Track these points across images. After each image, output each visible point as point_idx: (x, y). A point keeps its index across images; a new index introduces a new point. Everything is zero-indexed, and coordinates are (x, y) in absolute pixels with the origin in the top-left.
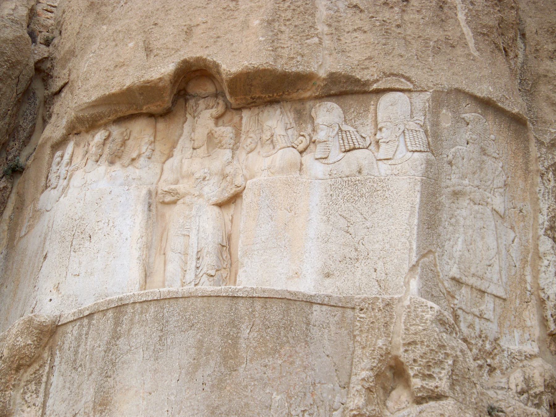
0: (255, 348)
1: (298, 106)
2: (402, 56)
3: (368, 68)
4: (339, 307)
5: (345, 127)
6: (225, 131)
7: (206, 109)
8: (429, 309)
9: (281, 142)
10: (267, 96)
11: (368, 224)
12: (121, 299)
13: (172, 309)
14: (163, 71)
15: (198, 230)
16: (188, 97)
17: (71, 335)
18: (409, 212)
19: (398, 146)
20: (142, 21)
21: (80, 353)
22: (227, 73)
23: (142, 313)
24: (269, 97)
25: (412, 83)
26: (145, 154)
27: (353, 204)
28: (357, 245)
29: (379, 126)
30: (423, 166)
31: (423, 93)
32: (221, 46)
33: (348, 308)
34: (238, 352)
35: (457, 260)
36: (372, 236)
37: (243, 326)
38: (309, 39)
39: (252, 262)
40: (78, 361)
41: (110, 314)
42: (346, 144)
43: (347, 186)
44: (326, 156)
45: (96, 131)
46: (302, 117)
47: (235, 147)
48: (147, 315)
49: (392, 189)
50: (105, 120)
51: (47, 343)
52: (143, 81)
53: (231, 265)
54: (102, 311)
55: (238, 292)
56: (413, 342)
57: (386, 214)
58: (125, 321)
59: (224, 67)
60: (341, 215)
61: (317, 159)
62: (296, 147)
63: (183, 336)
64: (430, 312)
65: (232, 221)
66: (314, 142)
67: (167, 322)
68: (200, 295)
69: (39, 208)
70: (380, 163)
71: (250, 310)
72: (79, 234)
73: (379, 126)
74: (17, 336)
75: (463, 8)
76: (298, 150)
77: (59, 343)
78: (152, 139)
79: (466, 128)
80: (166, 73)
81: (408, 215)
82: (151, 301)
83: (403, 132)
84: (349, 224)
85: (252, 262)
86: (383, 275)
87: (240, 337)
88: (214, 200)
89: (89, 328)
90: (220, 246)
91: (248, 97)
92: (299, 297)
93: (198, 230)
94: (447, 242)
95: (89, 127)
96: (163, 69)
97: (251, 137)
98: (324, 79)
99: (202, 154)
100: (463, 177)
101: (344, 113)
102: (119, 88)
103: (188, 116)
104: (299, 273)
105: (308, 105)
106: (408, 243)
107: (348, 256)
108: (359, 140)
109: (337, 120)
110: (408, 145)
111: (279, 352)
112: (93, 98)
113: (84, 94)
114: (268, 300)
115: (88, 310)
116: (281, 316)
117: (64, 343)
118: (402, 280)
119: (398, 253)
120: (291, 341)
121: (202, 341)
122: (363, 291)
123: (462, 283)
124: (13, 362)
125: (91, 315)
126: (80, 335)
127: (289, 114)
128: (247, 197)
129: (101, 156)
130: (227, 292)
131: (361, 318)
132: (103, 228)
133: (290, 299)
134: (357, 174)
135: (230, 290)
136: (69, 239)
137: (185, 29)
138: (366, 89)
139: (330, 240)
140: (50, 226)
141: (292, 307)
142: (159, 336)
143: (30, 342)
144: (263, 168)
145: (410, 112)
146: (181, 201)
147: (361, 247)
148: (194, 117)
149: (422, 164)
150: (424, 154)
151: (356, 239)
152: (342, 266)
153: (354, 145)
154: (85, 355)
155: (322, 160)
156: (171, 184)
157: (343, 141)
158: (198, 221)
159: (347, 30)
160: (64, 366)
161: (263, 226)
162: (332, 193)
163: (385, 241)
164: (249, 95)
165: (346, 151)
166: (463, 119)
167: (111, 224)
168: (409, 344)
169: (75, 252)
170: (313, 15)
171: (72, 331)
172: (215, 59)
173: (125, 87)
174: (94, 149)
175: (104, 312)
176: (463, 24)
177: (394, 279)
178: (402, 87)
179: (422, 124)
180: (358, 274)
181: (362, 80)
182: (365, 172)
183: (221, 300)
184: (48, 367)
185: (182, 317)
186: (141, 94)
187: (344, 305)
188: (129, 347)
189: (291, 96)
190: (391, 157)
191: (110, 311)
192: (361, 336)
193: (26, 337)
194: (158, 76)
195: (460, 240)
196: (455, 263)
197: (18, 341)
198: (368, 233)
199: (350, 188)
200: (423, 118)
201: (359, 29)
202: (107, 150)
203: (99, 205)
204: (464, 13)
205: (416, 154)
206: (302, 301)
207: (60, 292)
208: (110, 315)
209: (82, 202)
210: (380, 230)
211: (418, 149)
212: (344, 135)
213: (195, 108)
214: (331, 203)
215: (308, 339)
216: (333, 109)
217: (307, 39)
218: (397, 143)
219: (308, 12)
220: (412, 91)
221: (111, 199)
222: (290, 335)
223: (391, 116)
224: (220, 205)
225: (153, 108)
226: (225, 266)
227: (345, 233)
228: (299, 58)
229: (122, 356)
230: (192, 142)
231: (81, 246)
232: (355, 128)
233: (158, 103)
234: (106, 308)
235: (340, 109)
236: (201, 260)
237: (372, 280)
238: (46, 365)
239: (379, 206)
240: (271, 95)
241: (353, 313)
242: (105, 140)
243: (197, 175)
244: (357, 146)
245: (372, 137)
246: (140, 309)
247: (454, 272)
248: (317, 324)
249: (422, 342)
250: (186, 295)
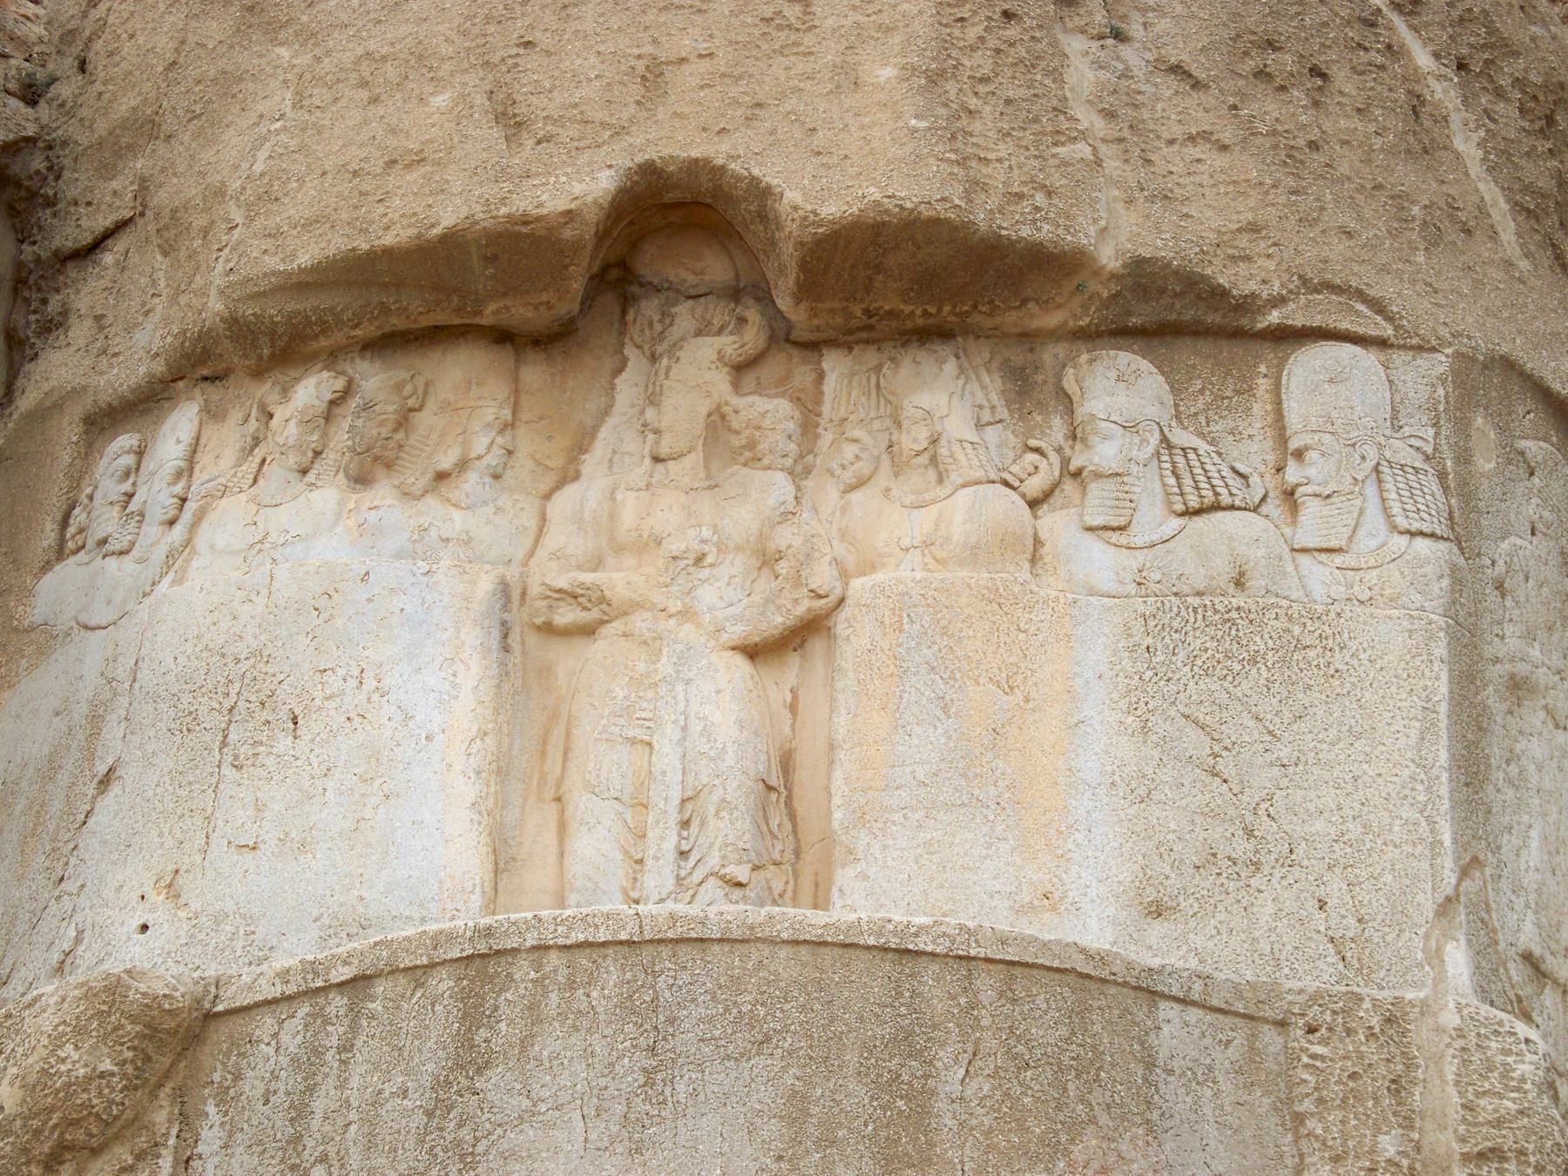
0: (988, 1133)
1: (1016, 355)
2: (1349, 235)
3: (1248, 258)
4: (1237, 1014)
5: (1180, 437)
6: (770, 412)
7: (699, 333)
8: (1523, 1046)
9: (967, 464)
10: (918, 312)
11: (1285, 753)
12: (488, 932)
13: (685, 977)
14: (578, 189)
15: (684, 729)
16: (635, 289)
17: (271, 1050)
18: (1417, 725)
19: (1362, 511)
20: (475, 30)
21: (319, 1115)
22: (805, 218)
23: (572, 985)
24: (926, 314)
25: (1390, 319)
26: (484, 462)
27: (1226, 684)
28: (1250, 818)
29: (1294, 444)
30: (1445, 582)
31: (1425, 355)
32: (773, 132)
33: (1265, 1020)
34: (931, 1144)
35: (1532, 897)
36: (1300, 793)
37: (941, 1054)
38: (1063, 144)
39: (885, 847)
40: (310, 1143)
41: (442, 983)
42: (1187, 489)
43: (1200, 623)
44: (1122, 521)
45: (293, 373)
46: (1030, 391)
47: (799, 468)
48: (594, 994)
49: (1353, 645)
50: (338, 337)
51: (167, 1075)
52: (509, 216)
53: (797, 853)
54: (406, 969)
55: (916, 935)
56: (1492, 1150)
57: (1342, 724)
58: (504, 1009)
59: (792, 196)
60: (1187, 717)
61: (1090, 529)
62: (1017, 484)
63: (733, 1074)
64: (1529, 1057)
65: (793, 708)
66: (1077, 474)
67: (671, 1021)
68: (785, 936)
69: (38, 619)
70: (1304, 560)
71: (963, 1001)
72: (244, 710)
73: (1294, 444)
74: (57, 1042)
75: (1472, 126)
76: (1023, 496)
77: (216, 1077)
78: (507, 413)
79: (1529, 485)
80: (589, 199)
81: (1414, 734)
82: (604, 944)
83: (1376, 469)
84: (1217, 749)
85: (885, 847)
86: (1352, 921)
87: (933, 1093)
88: (737, 632)
89: (354, 1028)
90: (761, 785)
91: (857, 310)
92: (1115, 970)
93: (684, 729)
94: (1506, 836)
95: (272, 356)
96: (576, 184)
97: (855, 441)
98: (1113, 276)
99: (687, 480)
100: (1529, 637)
101: (1175, 390)
102: (412, 232)
103: (630, 351)
104: (1057, 895)
105: (1050, 354)
106: (1424, 824)
107: (1223, 850)
108: (1230, 482)
109: (1153, 411)
110: (1394, 511)
111: (1067, 1153)
112: (304, 260)
113: (267, 244)
114: (1017, 971)
115: (345, 963)
116: (1064, 1031)
117: (238, 1077)
118: (1418, 942)
119: (1391, 852)
120: (1103, 1119)
121: (804, 1097)
122: (1287, 971)
123: (1545, 975)
124: (37, 1132)
125: (359, 984)
126: (317, 1052)
127: (986, 378)
128: (856, 634)
129: (317, 454)
130: (880, 934)
131: (1314, 1057)
132: (343, 693)
133: (1088, 976)
134: (1231, 589)
135: (891, 927)
136: (219, 720)
137: (640, 66)
138: (1245, 322)
139: (1155, 796)
140: (122, 672)
141: (1095, 1004)
142: (645, 1070)
143: (107, 1065)
144: (906, 542)
145: (1389, 408)
146: (617, 626)
147: (1264, 826)
148: (654, 358)
149: (1442, 576)
150: (1442, 545)
151: (1245, 798)
152: (1205, 881)
153: (1217, 494)
154: (340, 1122)
155: (1110, 533)
156: (579, 568)
157: (1178, 477)
158: (681, 696)
159: (1166, 135)
161: (918, 730)
162: (1149, 641)
163: (1346, 812)
164: (862, 301)
165: (1190, 513)
166: (1522, 453)
167: (370, 683)
168: (1481, 1155)
169: (238, 768)
170: (1056, 75)
171: (275, 1035)
172: (756, 172)
173: (436, 231)
174: (293, 429)
175: (418, 974)
176: (1475, 170)
177: (1389, 938)
178: (1361, 330)
179: (1429, 449)
180: (1265, 912)
181: (1235, 292)
182: (1256, 583)
183: (860, 962)
184: (170, 1159)
185: (726, 1009)
186: (491, 260)
187: (1252, 1010)
188: (526, 1103)
189: (998, 320)
190: (1343, 543)
191: (444, 972)
192: (1322, 1119)
193: (95, 1047)
194: (562, 204)
195: (1533, 833)
196: (1527, 906)
197: (63, 1060)
198: (1284, 783)
199: (1211, 631)
200: (1431, 432)
201: (1205, 136)
202: (341, 437)
203: (324, 616)
204: (1475, 137)
205: (1420, 543)
206: (1125, 984)
207: (182, 901)
208: (443, 986)
209: (260, 600)
210: (1326, 775)
211: (1425, 527)
212: (1180, 460)
213: (658, 327)
214: (1149, 673)
215: (1155, 1115)
216: (1138, 373)
217: (1055, 144)
218: (1358, 502)
219: (1043, 64)
220: (1392, 346)
221: (370, 600)
222: (1096, 1097)
223: (1334, 414)
224: (754, 652)
225: (522, 313)
226: (777, 856)
227: (1204, 776)
228: (1040, 199)
229: (499, 1131)
230: (651, 437)
231: (262, 749)
232: (1211, 444)
233: (545, 297)
234: (425, 961)
235: (1161, 378)
236: (694, 828)
237: (1315, 936)
238: (164, 1152)
239: (1315, 695)
240: (932, 310)
241: (1280, 1040)
242: (332, 403)
243: (675, 546)
244: (1225, 499)
245: (1268, 477)
246: (563, 973)
247: (1528, 937)
248: (1176, 1064)
249: (1522, 1152)
250: (736, 934)
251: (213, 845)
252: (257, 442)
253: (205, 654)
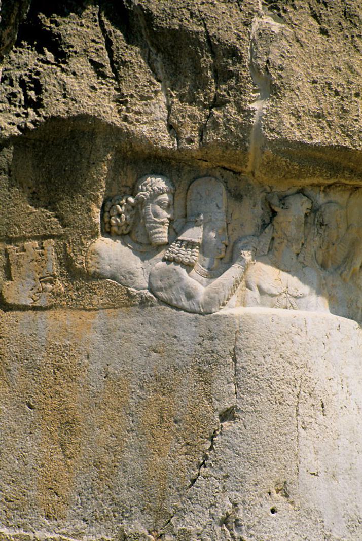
169: (304, 429)
251: (301, 472)
252: (264, 226)
253: (281, 360)
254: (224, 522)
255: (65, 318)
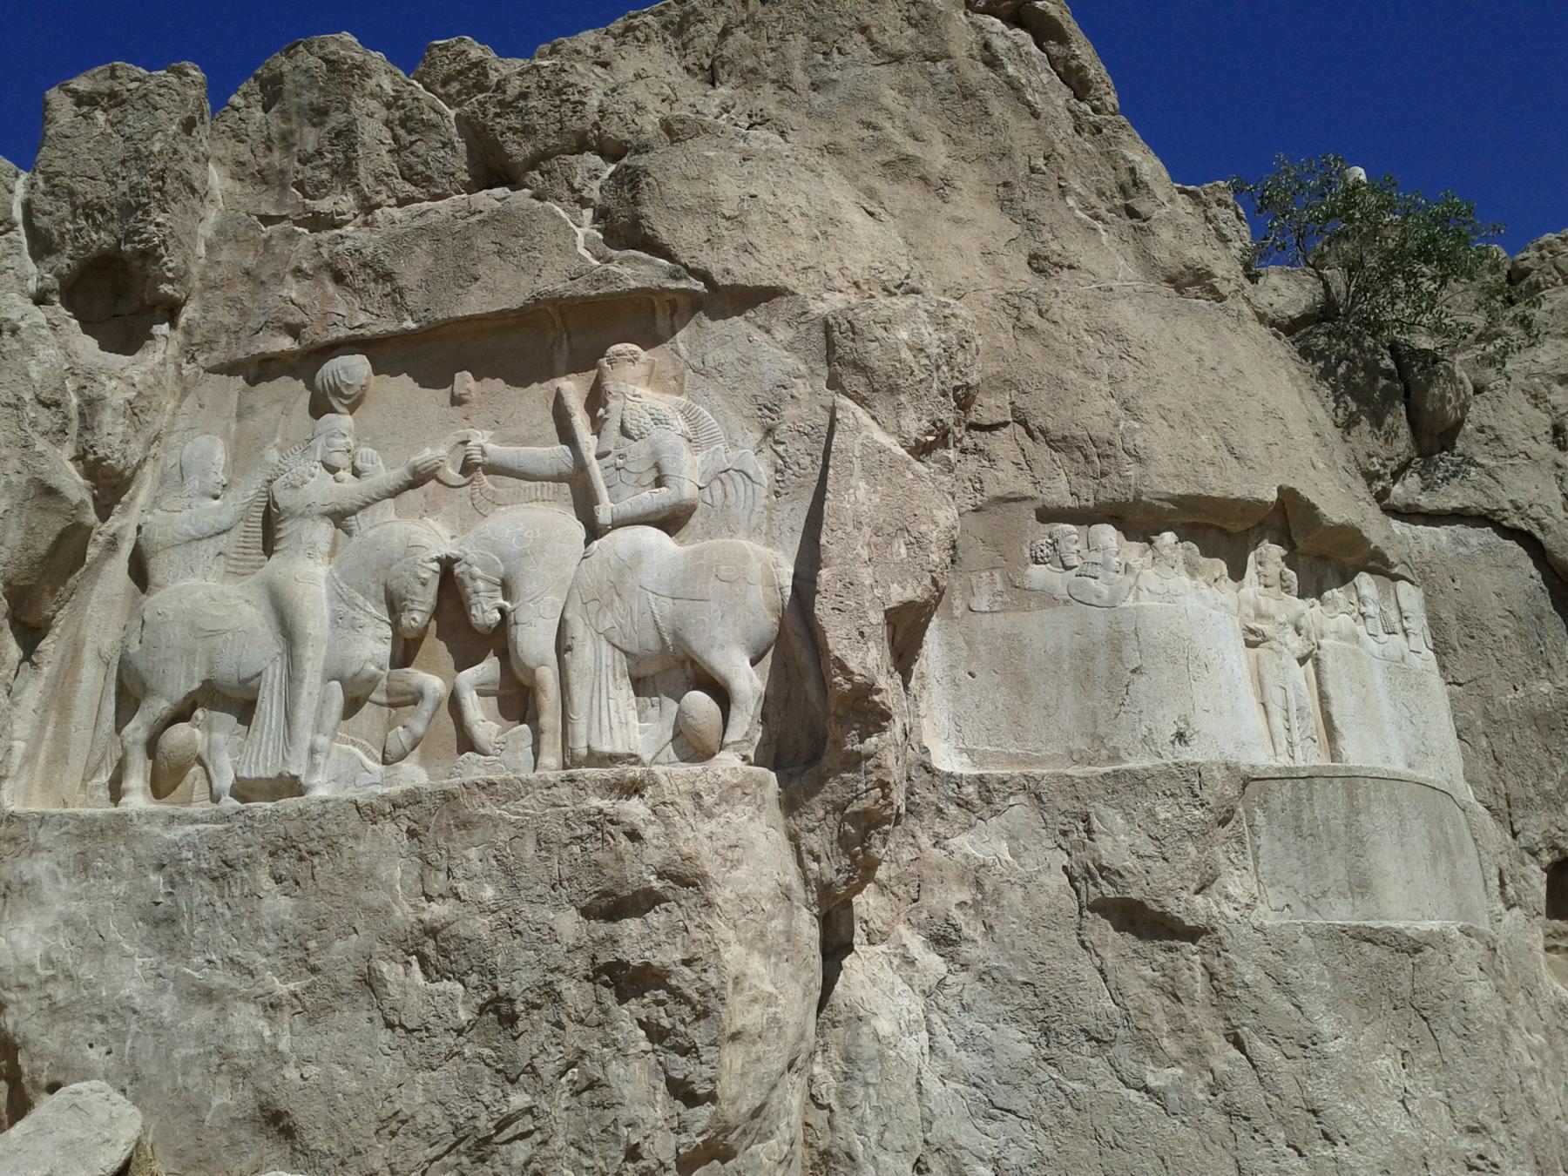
160: (1278, 832)
254: (1144, 740)
255: (1012, 617)
